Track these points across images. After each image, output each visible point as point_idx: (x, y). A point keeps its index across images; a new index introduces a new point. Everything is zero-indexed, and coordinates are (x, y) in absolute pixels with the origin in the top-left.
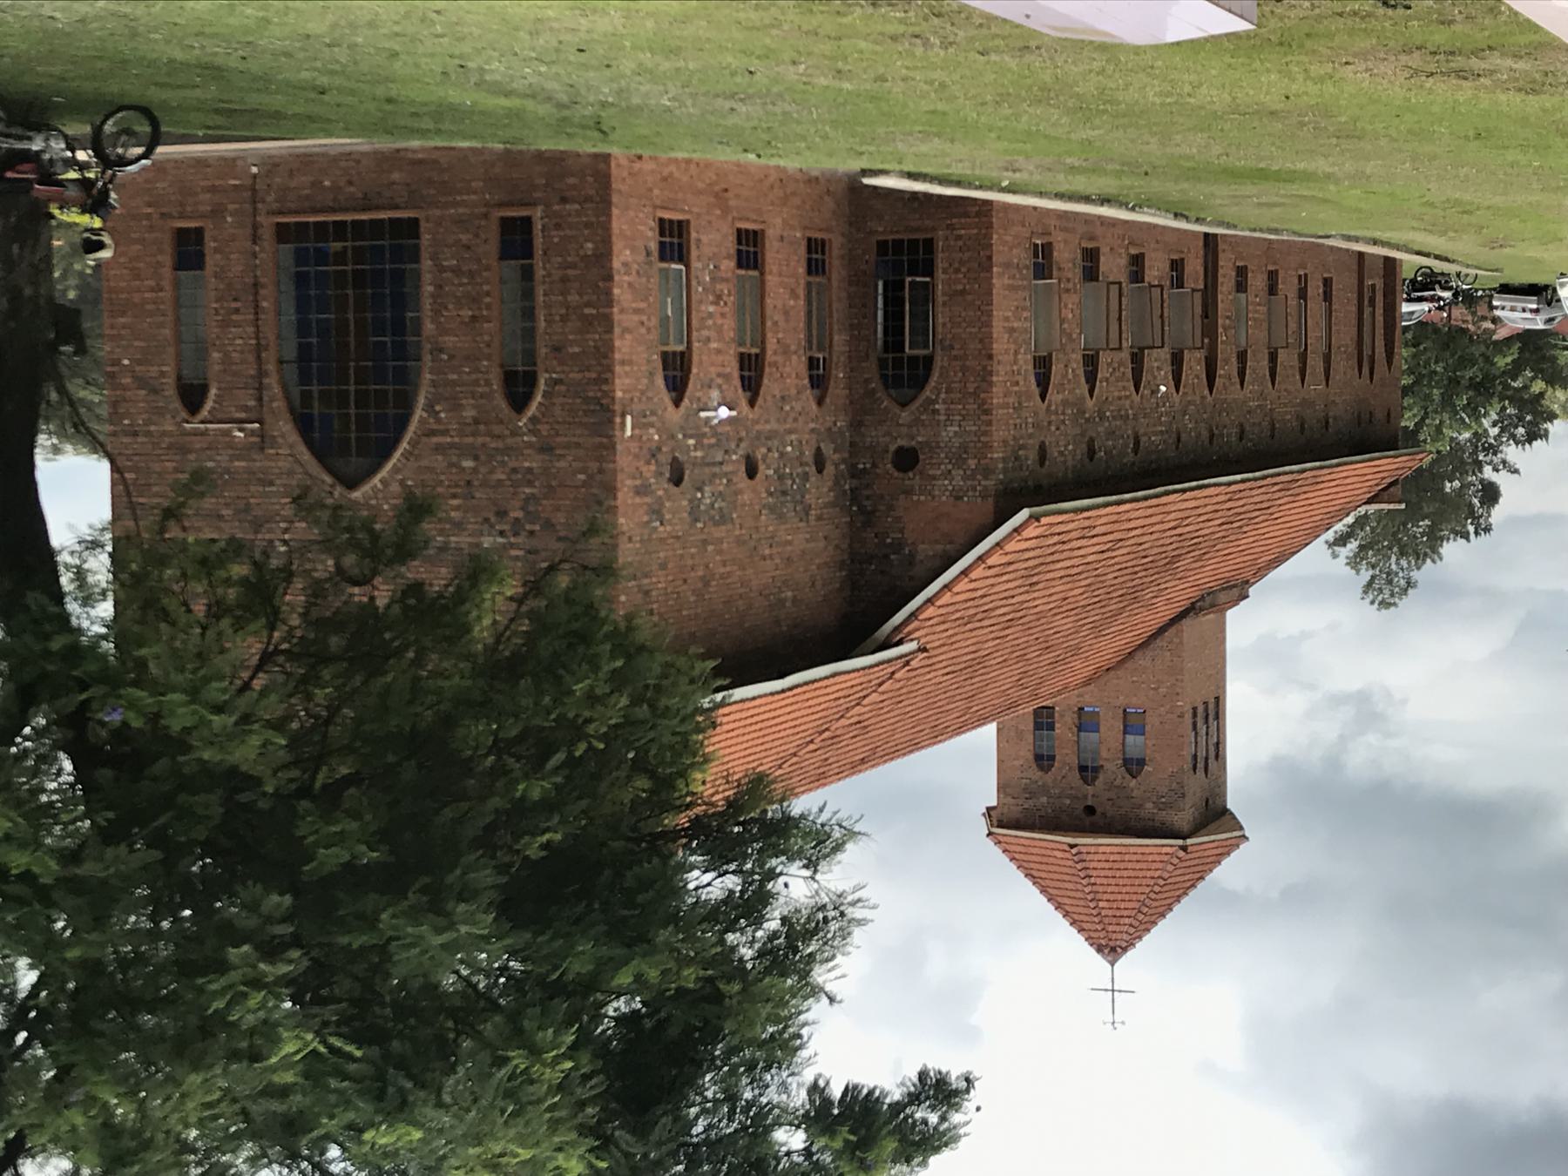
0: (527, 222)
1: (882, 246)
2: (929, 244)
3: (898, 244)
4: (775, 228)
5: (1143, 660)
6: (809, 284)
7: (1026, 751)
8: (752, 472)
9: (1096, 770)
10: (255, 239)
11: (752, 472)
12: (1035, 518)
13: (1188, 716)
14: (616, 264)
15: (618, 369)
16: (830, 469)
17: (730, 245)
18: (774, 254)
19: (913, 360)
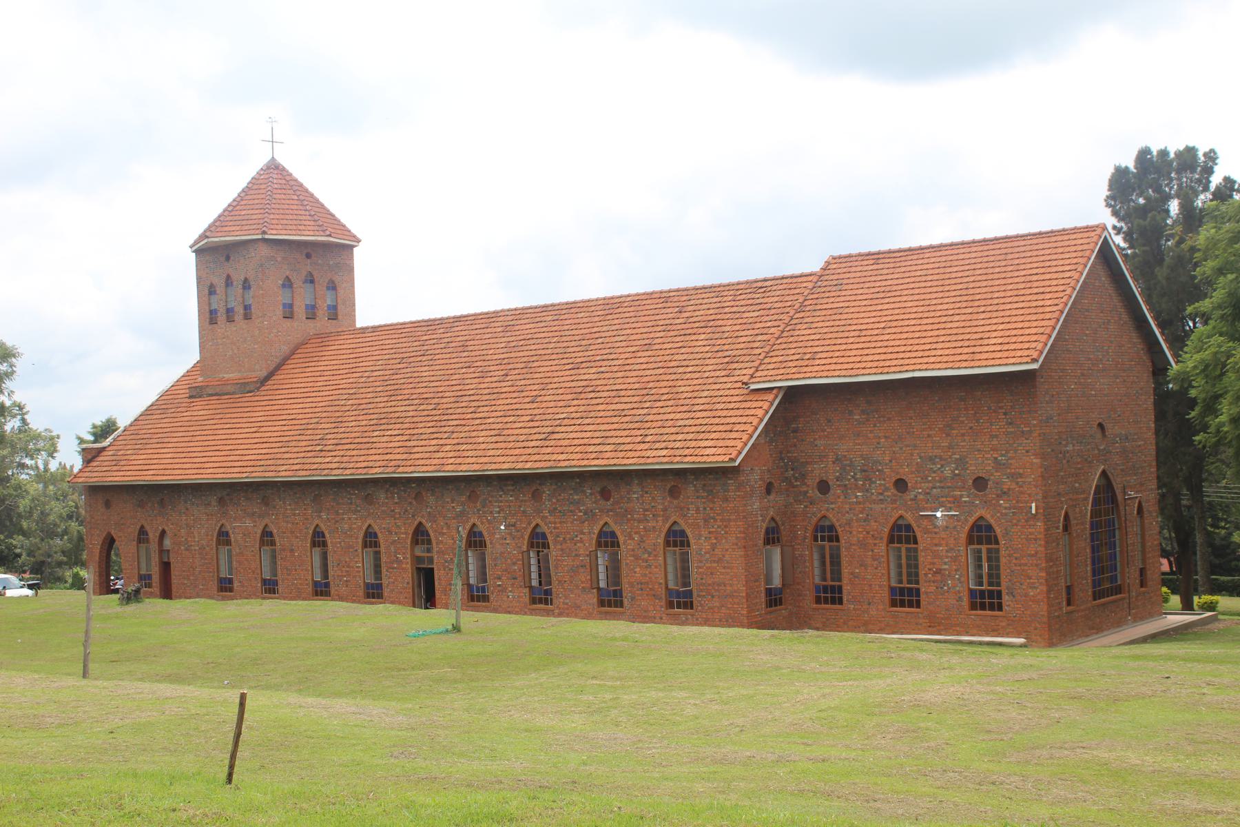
5: (285, 349)
7: (341, 292)
9: (305, 282)
11: (901, 485)
14: (1045, 588)
15: (1042, 536)
16: (812, 482)
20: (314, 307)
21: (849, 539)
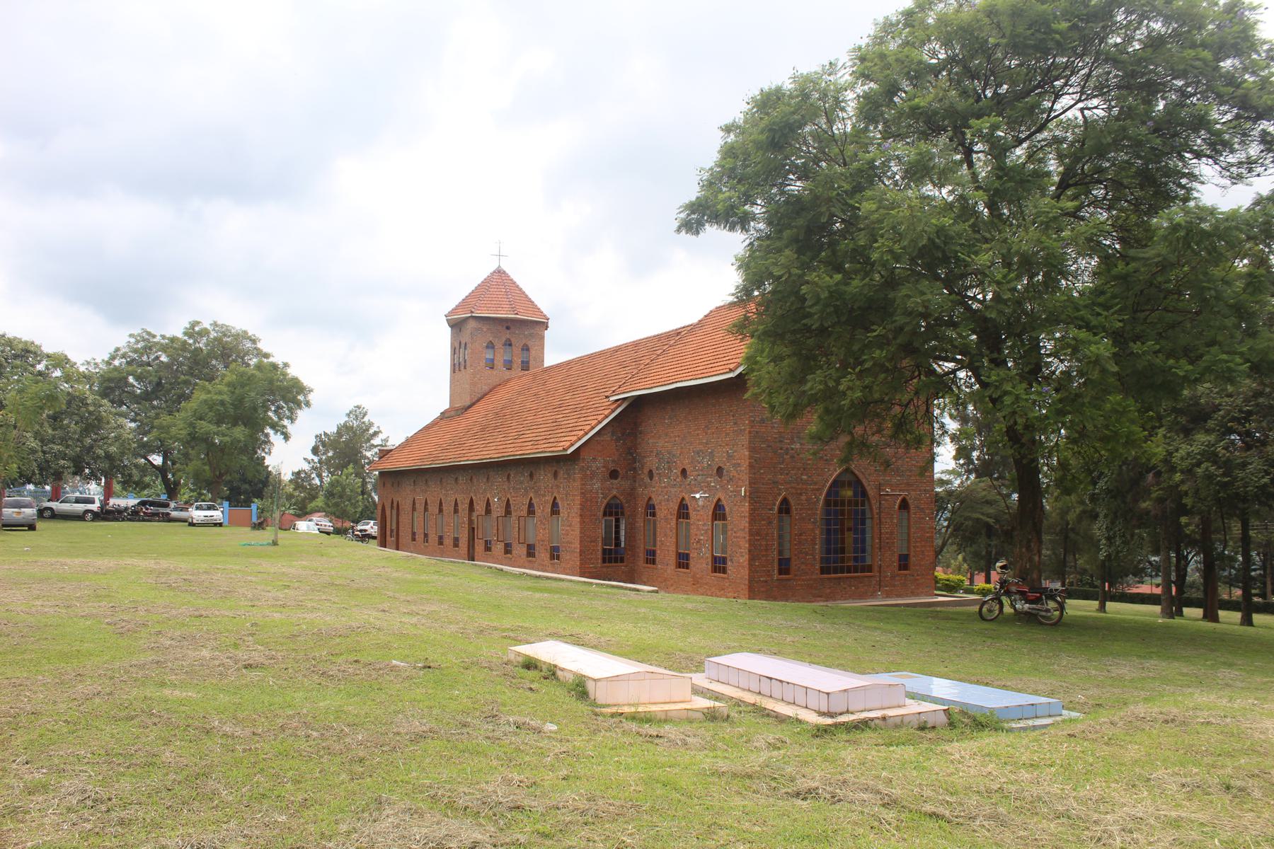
0: (780, 573)
1: (622, 560)
2: (604, 561)
3: (616, 561)
4: (671, 568)
5: (486, 388)
6: (655, 544)
7: (533, 352)
8: (684, 472)
10: (880, 567)
11: (684, 472)
12: (565, 450)
13: (468, 364)
16: (646, 471)
17: (692, 563)
18: (672, 559)
19: (611, 515)
20: (510, 362)
21: (661, 514)
